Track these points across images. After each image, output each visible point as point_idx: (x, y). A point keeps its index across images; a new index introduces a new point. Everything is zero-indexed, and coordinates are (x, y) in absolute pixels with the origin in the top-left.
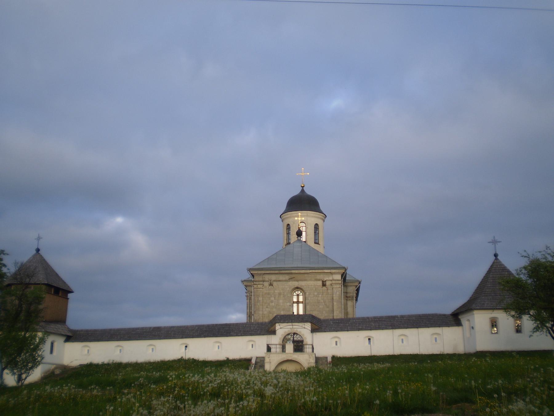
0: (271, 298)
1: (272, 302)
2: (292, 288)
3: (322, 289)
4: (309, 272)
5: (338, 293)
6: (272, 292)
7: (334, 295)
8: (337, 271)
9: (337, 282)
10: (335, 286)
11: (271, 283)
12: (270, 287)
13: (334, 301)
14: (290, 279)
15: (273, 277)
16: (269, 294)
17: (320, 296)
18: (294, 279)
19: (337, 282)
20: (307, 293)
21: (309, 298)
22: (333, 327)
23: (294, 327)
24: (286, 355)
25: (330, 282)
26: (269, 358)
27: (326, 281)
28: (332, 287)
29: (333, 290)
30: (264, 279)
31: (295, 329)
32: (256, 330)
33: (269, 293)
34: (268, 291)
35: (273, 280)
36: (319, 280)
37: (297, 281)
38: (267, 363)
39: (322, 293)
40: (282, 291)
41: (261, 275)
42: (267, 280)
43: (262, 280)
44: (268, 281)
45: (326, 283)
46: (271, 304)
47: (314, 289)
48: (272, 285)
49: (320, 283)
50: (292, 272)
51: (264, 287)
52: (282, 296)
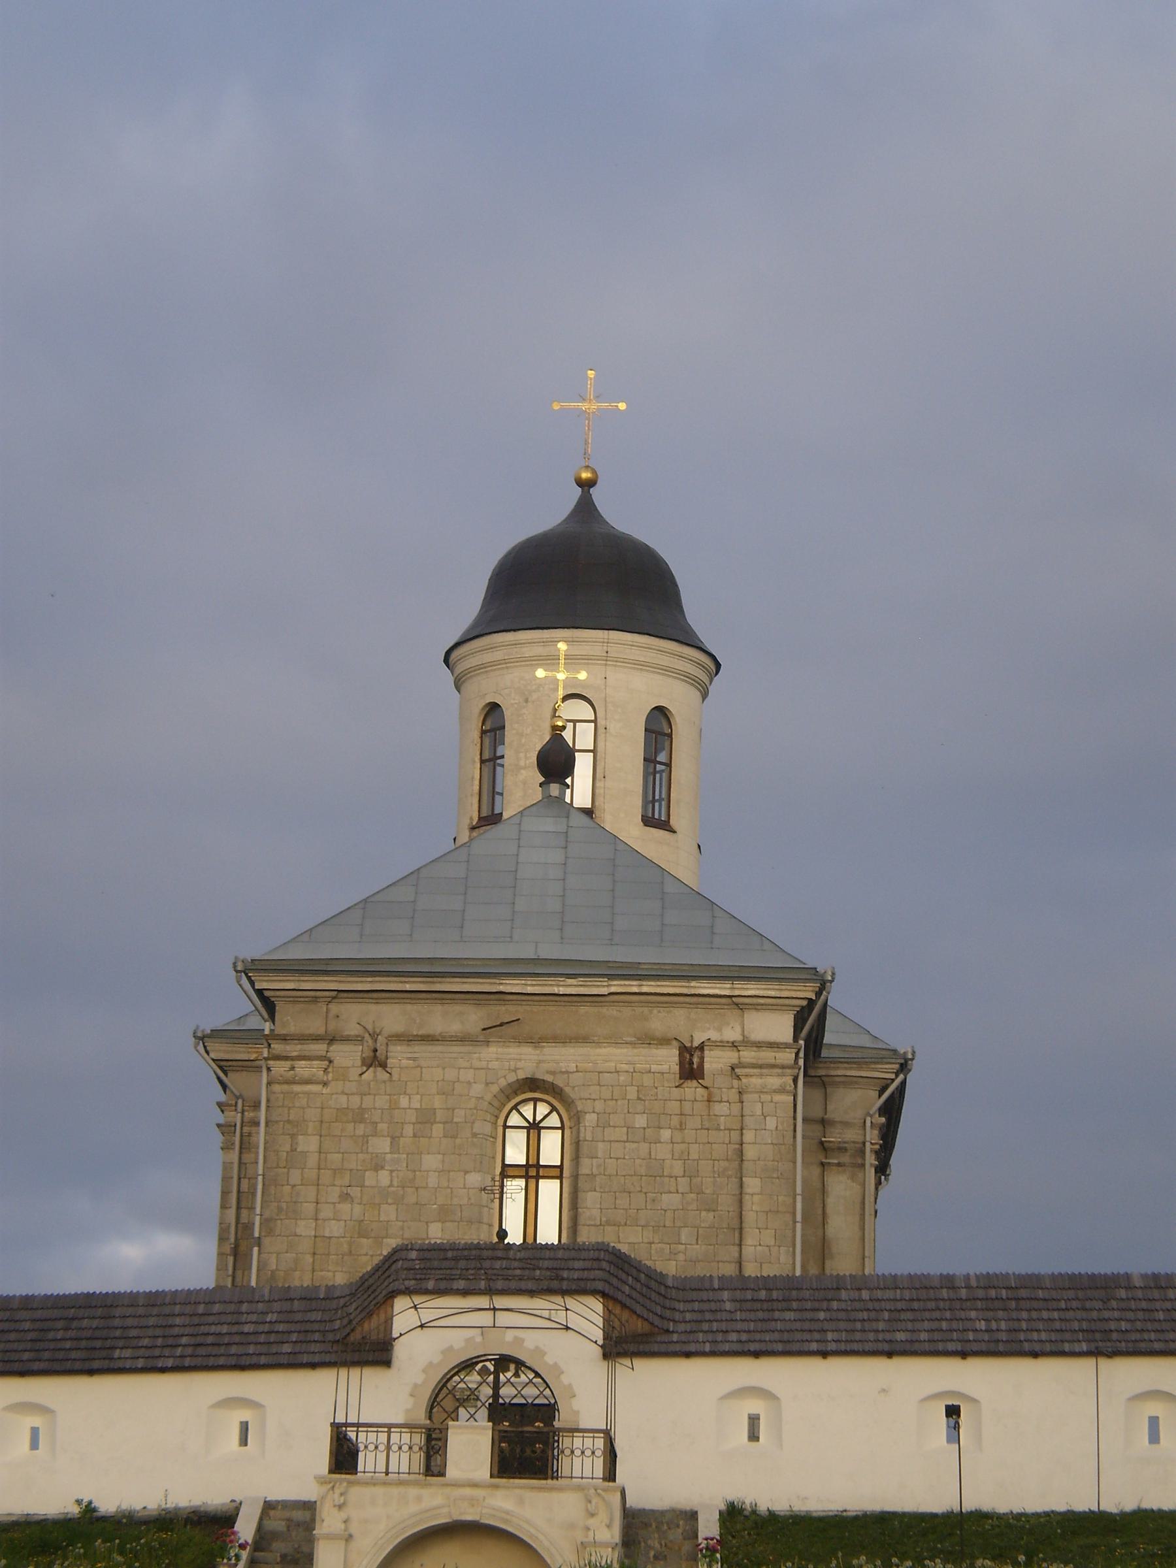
0: (373, 1141)
3: (676, 1093)
4: (604, 991)
5: (771, 1123)
7: (749, 1136)
8: (773, 993)
9: (768, 1056)
10: (756, 1082)
14: (494, 1031)
17: (666, 1134)
18: (508, 1030)
19: (768, 1056)
21: (600, 1145)
22: (739, 1326)
23: (504, 1319)
24: (448, 1490)
25: (730, 1057)
26: (340, 1507)
27: (701, 1047)
28: (735, 1083)
30: (332, 1026)
31: (510, 1335)
32: (272, 1338)
35: (386, 1033)
36: (664, 1041)
37: (536, 1041)
38: (331, 1537)
39: (675, 1121)
40: (438, 1103)
41: (315, 1000)
42: (353, 1029)
43: (322, 1031)
44: (358, 1039)
45: (702, 1059)
47: (632, 1093)
48: (383, 1065)
49: (668, 1058)
50: (502, 988)
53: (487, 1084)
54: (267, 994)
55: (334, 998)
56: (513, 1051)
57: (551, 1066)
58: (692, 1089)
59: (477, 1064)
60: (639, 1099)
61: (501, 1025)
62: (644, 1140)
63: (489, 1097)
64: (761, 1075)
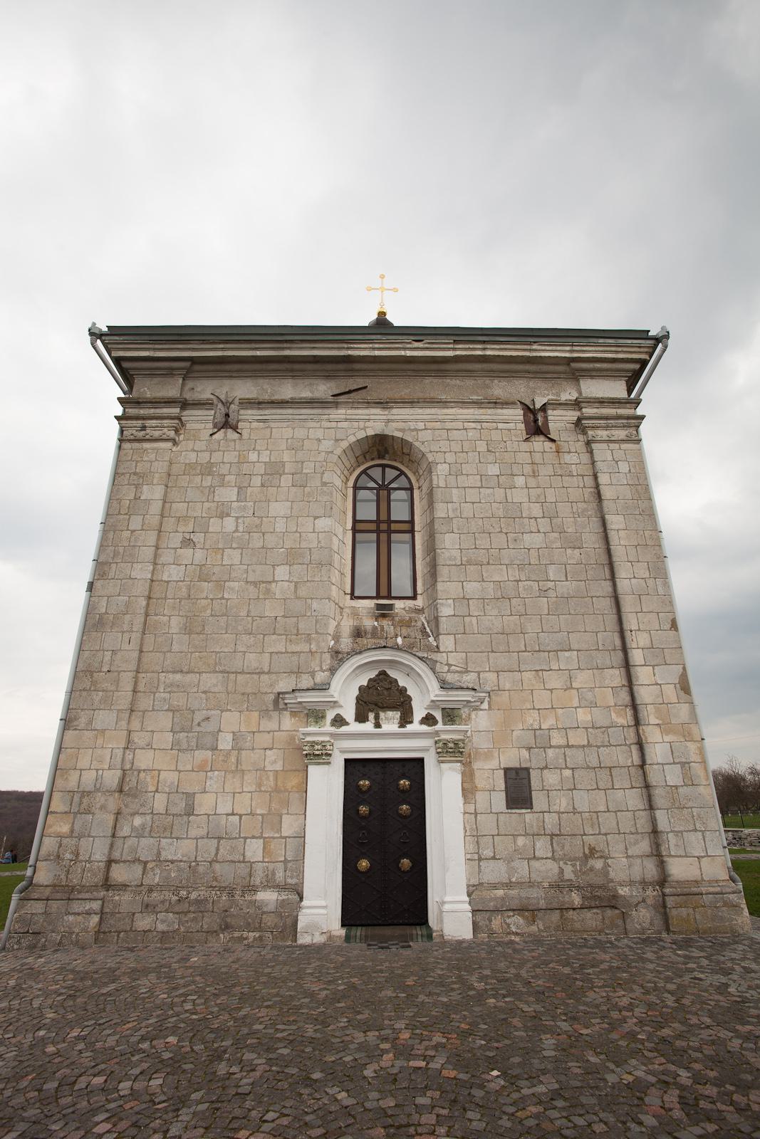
1: (223, 515)
2: (352, 439)
3: (525, 446)
6: (231, 457)
7: (603, 479)
10: (602, 434)
11: (227, 415)
13: (605, 503)
15: (243, 389)
16: (208, 470)
17: (520, 481)
20: (442, 469)
21: (454, 491)
27: (544, 408)
29: (591, 452)
33: (210, 464)
34: (207, 455)
37: (383, 404)
39: (528, 469)
40: (286, 457)
41: (170, 373)
45: (546, 418)
46: (215, 525)
47: (482, 447)
50: (350, 352)
51: (182, 437)
52: (286, 481)
54: (125, 365)
57: (401, 425)
58: (539, 443)
60: (488, 451)
63: (339, 451)
64: (607, 428)
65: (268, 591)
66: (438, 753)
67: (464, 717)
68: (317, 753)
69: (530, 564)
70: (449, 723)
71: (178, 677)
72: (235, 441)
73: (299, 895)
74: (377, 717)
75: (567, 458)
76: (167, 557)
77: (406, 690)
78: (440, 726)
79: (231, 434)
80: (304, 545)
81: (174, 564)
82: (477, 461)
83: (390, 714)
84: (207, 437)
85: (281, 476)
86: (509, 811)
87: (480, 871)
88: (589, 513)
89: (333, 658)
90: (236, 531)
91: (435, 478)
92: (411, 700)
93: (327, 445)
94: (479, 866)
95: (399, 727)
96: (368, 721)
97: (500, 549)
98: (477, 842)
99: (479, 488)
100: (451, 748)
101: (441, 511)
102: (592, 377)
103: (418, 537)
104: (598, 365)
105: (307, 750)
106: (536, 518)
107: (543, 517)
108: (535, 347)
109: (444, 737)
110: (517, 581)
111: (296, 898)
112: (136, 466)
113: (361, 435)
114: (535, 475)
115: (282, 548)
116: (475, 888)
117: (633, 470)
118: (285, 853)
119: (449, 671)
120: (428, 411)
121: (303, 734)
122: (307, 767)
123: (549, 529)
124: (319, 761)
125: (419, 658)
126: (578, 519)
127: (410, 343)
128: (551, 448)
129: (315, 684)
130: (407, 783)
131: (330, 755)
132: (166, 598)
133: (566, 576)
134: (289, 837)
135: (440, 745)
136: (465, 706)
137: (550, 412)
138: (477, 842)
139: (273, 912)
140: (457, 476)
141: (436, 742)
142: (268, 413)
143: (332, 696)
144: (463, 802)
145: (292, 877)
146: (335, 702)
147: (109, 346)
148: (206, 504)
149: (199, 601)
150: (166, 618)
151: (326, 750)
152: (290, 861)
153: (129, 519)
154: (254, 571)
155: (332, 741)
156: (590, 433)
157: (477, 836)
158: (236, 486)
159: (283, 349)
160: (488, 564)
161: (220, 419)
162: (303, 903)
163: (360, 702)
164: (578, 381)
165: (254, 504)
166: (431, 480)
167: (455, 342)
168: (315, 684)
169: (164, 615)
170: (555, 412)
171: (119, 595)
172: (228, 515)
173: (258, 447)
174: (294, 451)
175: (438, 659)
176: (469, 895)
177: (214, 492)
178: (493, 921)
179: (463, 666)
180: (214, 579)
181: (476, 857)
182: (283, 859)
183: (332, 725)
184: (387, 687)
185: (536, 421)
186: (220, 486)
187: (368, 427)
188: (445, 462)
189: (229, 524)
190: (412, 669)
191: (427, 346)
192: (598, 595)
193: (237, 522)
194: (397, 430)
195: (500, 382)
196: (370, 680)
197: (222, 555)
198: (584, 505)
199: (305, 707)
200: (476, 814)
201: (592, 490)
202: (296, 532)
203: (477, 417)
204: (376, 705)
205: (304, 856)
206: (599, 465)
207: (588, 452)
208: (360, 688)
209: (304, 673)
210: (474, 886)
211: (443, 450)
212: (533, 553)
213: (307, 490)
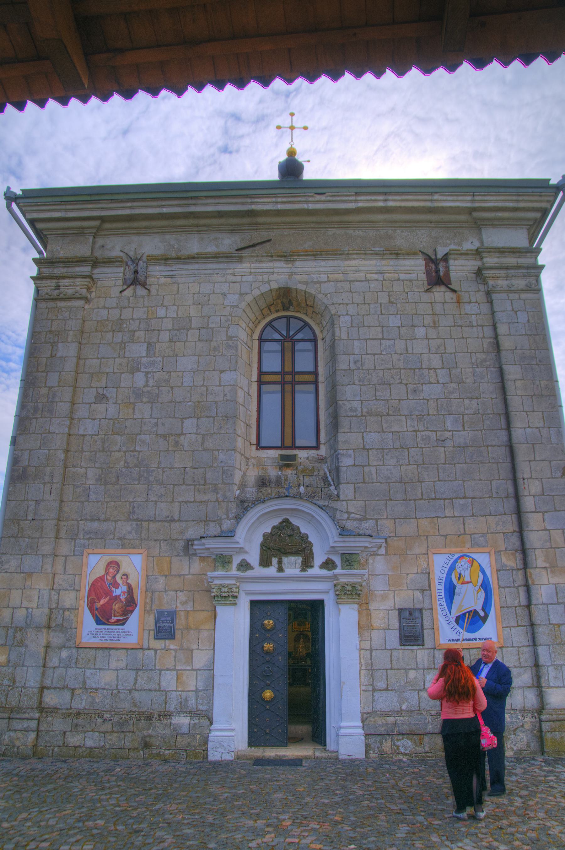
1: (134, 369)
2: (257, 293)
3: (426, 297)
7: (502, 329)
10: (502, 283)
11: (136, 272)
12: (129, 292)
13: (503, 353)
17: (420, 332)
20: (344, 321)
21: (356, 343)
27: (445, 259)
29: (491, 302)
33: (121, 320)
34: (117, 312)
36: (411, 254)
39: (428, 320)
40: (193, 312)
41: (81, 232)
45: (447, 268)
46: (126, 381)
47: (384, 298)
48: (144, 285)
50: (253, 207)
51: (93, 295)
53: (241, 294)
54: (40, 226)
55: (99, 229)
56: (266, 266)
57: (304, 278)
58: (439, 293)
59: (231, 278)
61: (254, 245)
62: (400, 337)
63: (243, 305)
64: (507, 277)
65: (177, 443)
66: (337, 595)
67: (362, 561)
68: (224, 594)
69: (428, 415)
70: (347, 567)
71: (96, 524)
72: (143, 297)
73: (209, 719)
74: (280, 562)
75: (468, 308)
76: (82, 411)
77: (307, 536)
78: (338, 571)
79: (140, 291)
80: (210, 398)
81: (89, 418)
82: (379, 313)
83: (292, 559)
84: (117, 294)
85: (188, 330)
86: (403, 647)
87: (373, 701)
88: (488, 363)
89: (239, 507)
90: (147, 385)
91: (337, 330)
92: (312, 546)
93: (232, 299)
94: (373, 696)
95: (301, 571)
96: (272, 565)
97: (399, 400)
98: (372, 676)
99: (380, 339)
100: (349, 591)
101: (343, 363)
102: (494, 226)
103: (321, 387)
104: (499, 214)
105: (215, 592)
106: (435, 369)
107: (443, 368)
108: (436, 197)
109: (343, 580)
110: (416, 431)
111: (206, 722)
112: (51, 325)
113: (265, 288)
114: (435, 325)
115: (190, 401)
116: (368, 715)
117: (531, 320)
118: (197, 683)
119: (348, 519)
120: (331, 263)
121: (211, 577)
122: (215, 607)
123: (447, 379)
124: (225, 602)
125: (319, 507)
126: (477, 370)
127: (312, 196)
128: (452, 299)
129: (222, 531)
130: (271, 622)
131: (236, 597)
132: (82, 451)
133: (463, 426)
134: (200, 670)
135: (339, 587)
136: (362, 551)
137: (451, 262)
138: (372, 676)
139: (186, 734)
140: (359, 328)
141: (335, 585)
142: (177, 268)
143: (237, 543)
144: (359, 639)
145: (203, 705)
146: (241, 548)
147: (24, 209)
148: (117, 360)
149: (113, 454)
150: (83, 470)
151: (232, 592)
152: (201, 691)
153: (46, 377)
154: (163, 424)
155: (238, 584)
156: (491, 282)
157: (372, 670)
158: (145, 342)
159: (188, 205)
160: (388, 414)
161: (130, 276)
162: (212, 726)
163: (264, 548)
164: (480, 229)
165: (163, 359)
166: (333, 333)
167: (357, 194)
168: (222, 531)
169: (81, 467)
170: (456, 262)
171: (40, 449)
172: (138, 370)
173: (166, 303)
174: (200, 306)
175: (338, 507)
176: (363, 721)
177: (125, 348)
178: (384, 744)
179: (362, 513)
180: (126, 432)
181: (370, 688)
182: (194, 688)
183: (238, 569)
184: (289, 533)
185: (437, 271)
186: (129, 342)
187: (272, 281)
188: (347, 314)
189: (140, 379)
190: (313, 516)
191: (329, 198)
192: (494, 443)
193: (147, 378)
194: (300, 282)
195: (402, 232)
196: (274, 527)
197: (134, 409)
198: (483, 356)
199: (212, 553)
200: (371, 650)
201: (491, 340)
202: (203, 385)
203: (379, 268)
204: (279, 550)
205: (213, 687)
206: (499, 315)
207: (488, 302)
208: (264, 536)
209: (211, 521)
210: (368, 713)
211: (346, 301)
212: (432, 404)
213: (213, 344)
